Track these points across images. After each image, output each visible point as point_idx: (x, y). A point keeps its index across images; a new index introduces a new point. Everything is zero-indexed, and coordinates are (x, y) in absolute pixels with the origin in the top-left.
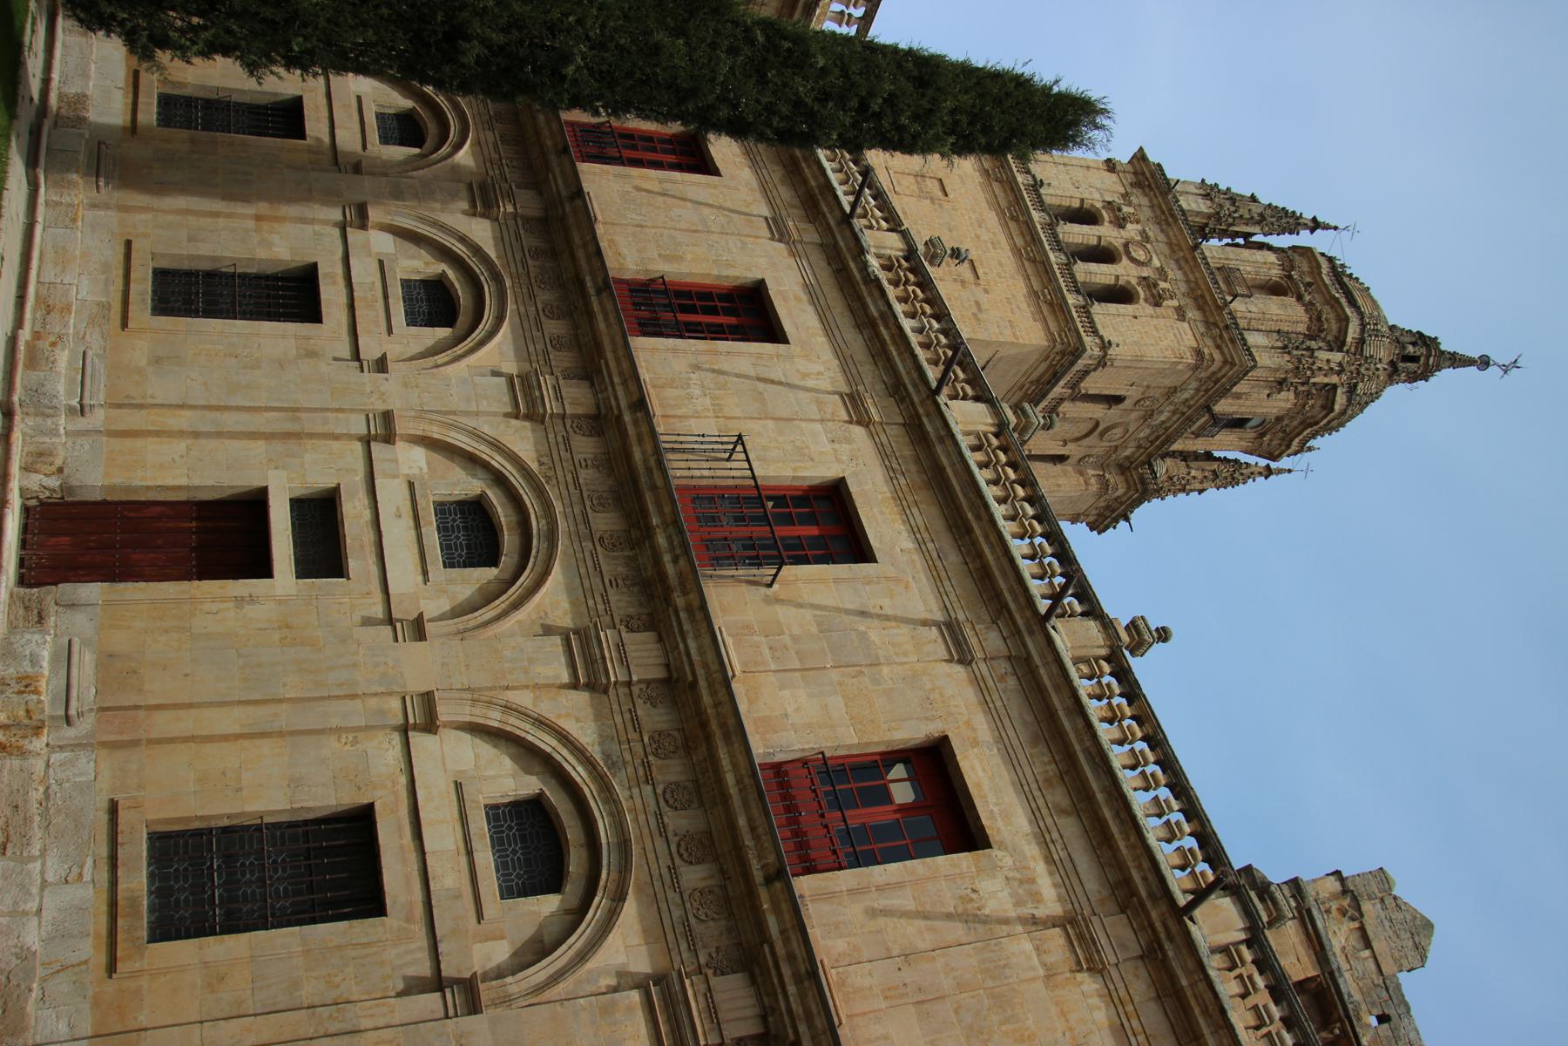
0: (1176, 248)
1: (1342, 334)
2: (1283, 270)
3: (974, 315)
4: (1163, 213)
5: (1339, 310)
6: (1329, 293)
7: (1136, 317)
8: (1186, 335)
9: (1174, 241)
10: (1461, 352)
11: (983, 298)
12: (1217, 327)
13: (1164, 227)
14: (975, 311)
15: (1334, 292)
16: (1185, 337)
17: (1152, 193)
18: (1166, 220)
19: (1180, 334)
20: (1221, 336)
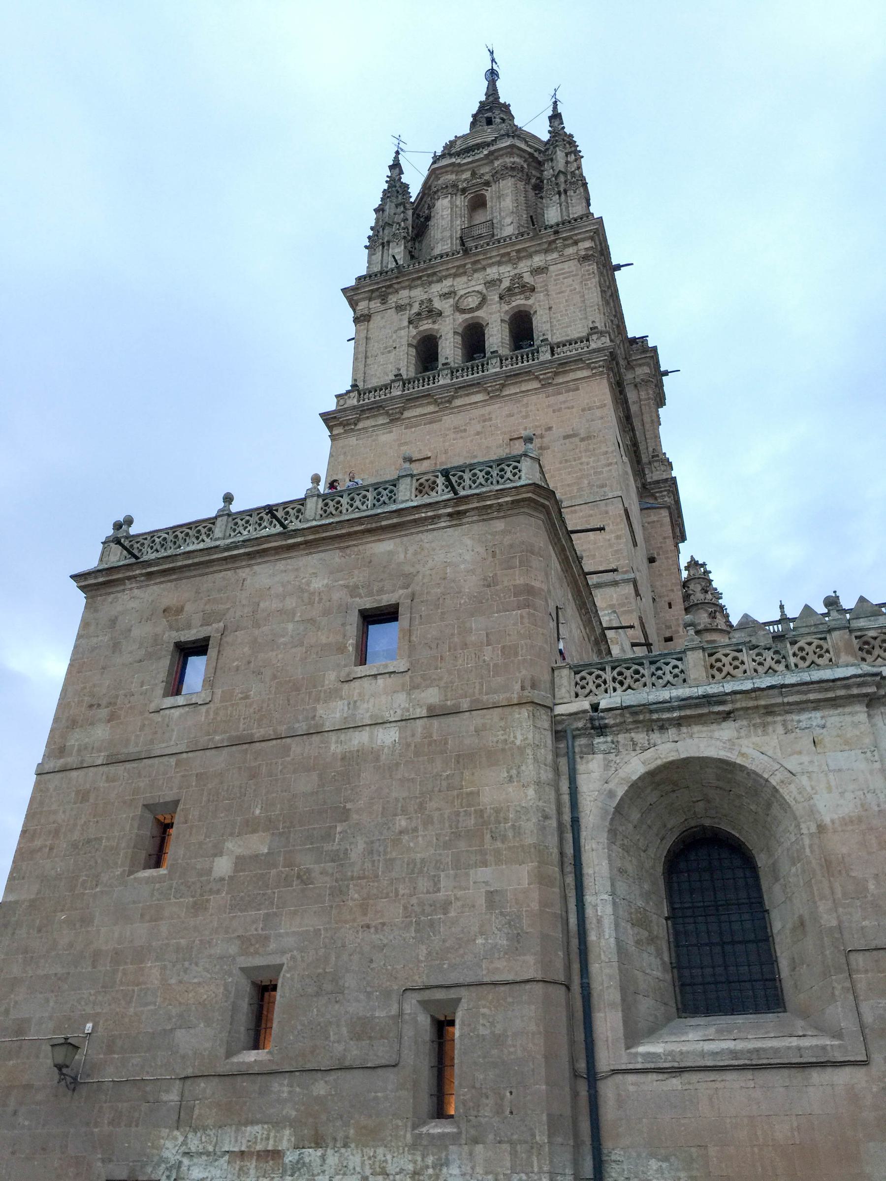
0: (461, 270)
1: (524, 154)
2: (456, 194)
3: (582, 440)
4: (420, 278)
5: (501, 153)
6: (481, 159)
7: (550, 308)
8: (563, 269)
9: (454, 271)
10: (485, 90)
11: (558, 431)
12: (554, 241)
13: (435, 278)
14: (577, 439)
15: (482, 156)
16: (567, 270)
17: (396, 286)
18: (429, 276)
19: (563, 274)
20: (565, 239)
